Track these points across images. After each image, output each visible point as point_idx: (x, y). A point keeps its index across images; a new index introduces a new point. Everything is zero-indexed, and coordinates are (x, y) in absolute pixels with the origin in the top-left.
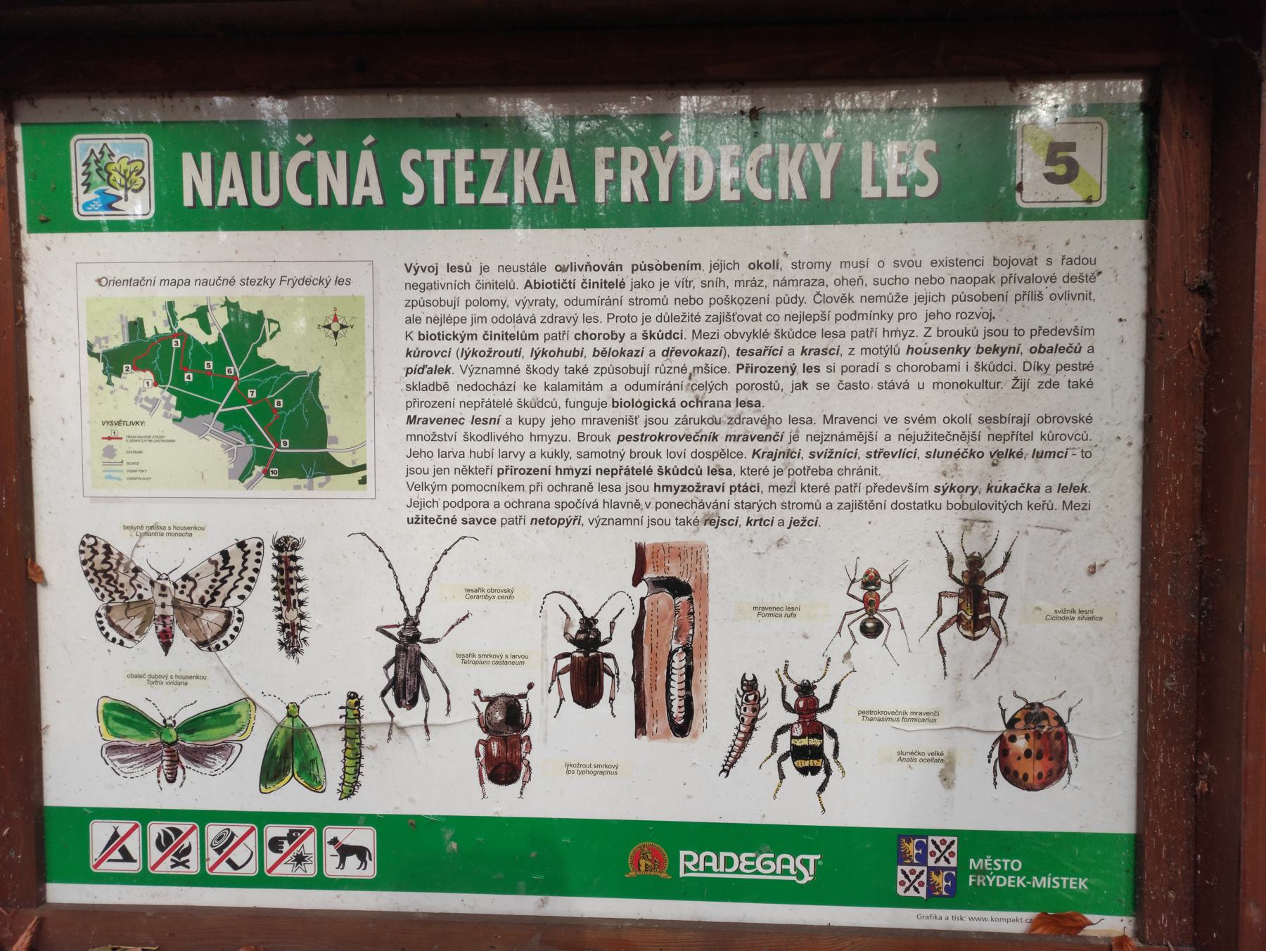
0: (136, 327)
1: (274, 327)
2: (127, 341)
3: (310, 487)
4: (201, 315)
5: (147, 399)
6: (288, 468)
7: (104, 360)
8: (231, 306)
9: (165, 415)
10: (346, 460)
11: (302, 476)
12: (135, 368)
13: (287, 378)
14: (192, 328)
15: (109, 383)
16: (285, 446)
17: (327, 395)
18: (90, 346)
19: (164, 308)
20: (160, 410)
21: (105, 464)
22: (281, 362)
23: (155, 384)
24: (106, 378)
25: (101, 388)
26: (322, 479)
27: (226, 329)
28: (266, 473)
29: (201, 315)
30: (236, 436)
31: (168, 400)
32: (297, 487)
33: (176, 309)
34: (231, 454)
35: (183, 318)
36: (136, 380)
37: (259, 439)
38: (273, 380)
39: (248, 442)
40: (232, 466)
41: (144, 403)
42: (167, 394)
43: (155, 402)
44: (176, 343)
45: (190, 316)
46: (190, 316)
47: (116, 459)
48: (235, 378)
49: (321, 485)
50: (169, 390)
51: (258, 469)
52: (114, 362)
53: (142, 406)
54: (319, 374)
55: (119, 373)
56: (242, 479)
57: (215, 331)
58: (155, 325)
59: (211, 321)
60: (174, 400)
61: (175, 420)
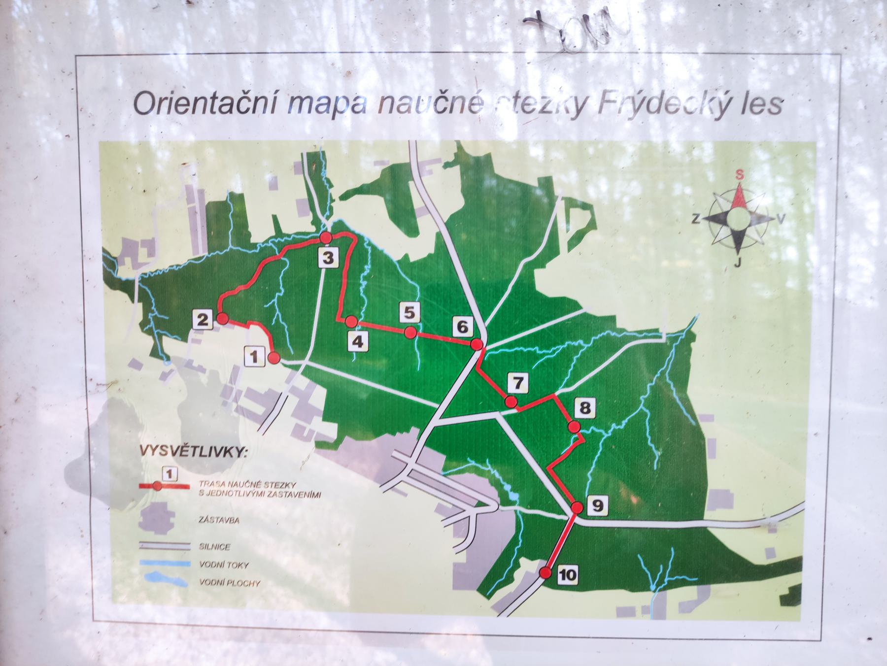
0: (224, 217)
1: (579, 219)
2: (203, 252)
3: (659, 613)
4: (394, 187)
5: (251, 394)
6: (608, 565)
7: (143, 298)
8: (474, 169)
9: (298, 432)
10: (751, 547)
11: (637, 584)
12: (222, 318)
13: (612, 345)
14: (369, 218)
15: (157, 352)
16: (597, 516)
17: (704, 393)
18: (110, 263)
19: (298, 168)
20: (286, 420)
21: (144, 545)
22: (593, 305)
23: (273, 359)
24: (148, 342)
25: (136, 365)
26: (689, 592)
27: (452, 223)
28: (549, 577)
29: (394, 187)
30: (475, 484)
31: (304, 397)
32: (625, 612)
33: (330, 172)
34: (461, 526)
35: (345, 197)
36: (225, 348)
37: (537, 497)
38: (567, 355)
39: (505, 501)
40: (462, 558)
41: (244, 402)
42: (302, 382)
43: (273, 402)
44: (328, 258)
45: (362, 190)
46: (362, 190)
47: (172, 535)
48: (474, 343)
49: (686, 608)
50: (308, 372)
51: (529, 567)
52: (168, 303)
53: (241, 410)
54: (690, 337)
55: (182, 332)
56: (486, 588)
57: (430, 228)
58: (276, 211)
59: (417, 203)
60: (319, 396)
61: (321, 445)
